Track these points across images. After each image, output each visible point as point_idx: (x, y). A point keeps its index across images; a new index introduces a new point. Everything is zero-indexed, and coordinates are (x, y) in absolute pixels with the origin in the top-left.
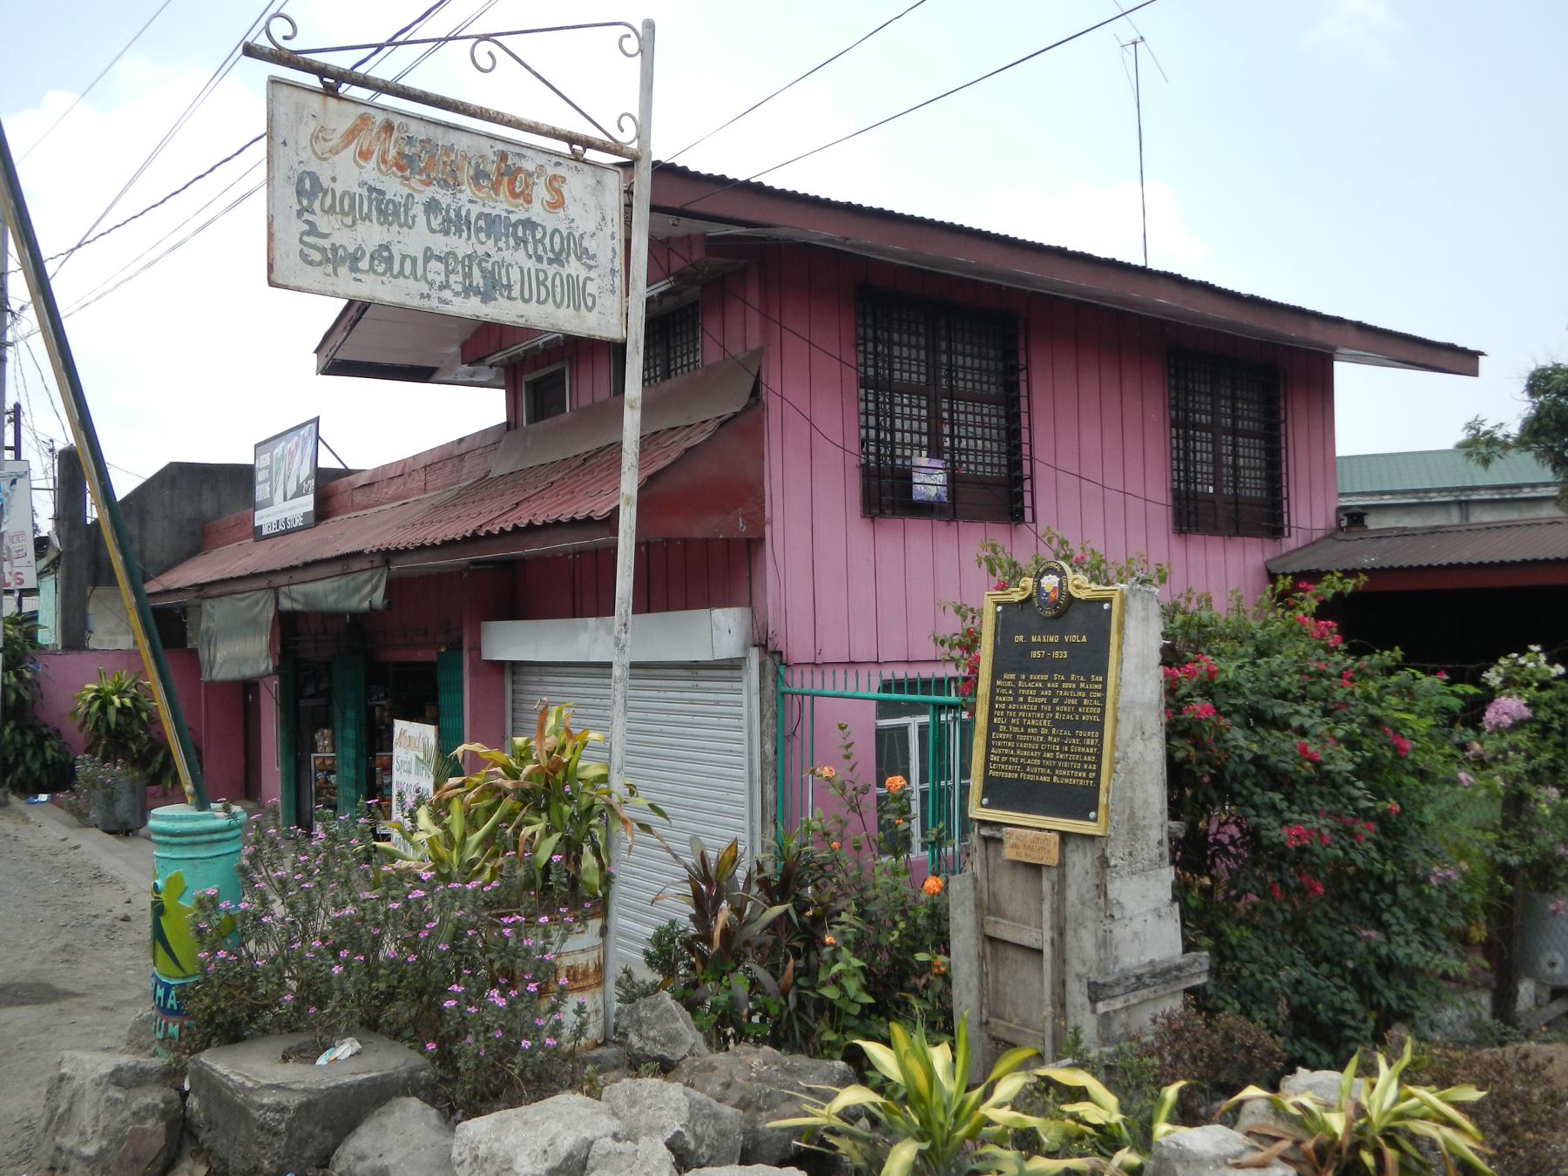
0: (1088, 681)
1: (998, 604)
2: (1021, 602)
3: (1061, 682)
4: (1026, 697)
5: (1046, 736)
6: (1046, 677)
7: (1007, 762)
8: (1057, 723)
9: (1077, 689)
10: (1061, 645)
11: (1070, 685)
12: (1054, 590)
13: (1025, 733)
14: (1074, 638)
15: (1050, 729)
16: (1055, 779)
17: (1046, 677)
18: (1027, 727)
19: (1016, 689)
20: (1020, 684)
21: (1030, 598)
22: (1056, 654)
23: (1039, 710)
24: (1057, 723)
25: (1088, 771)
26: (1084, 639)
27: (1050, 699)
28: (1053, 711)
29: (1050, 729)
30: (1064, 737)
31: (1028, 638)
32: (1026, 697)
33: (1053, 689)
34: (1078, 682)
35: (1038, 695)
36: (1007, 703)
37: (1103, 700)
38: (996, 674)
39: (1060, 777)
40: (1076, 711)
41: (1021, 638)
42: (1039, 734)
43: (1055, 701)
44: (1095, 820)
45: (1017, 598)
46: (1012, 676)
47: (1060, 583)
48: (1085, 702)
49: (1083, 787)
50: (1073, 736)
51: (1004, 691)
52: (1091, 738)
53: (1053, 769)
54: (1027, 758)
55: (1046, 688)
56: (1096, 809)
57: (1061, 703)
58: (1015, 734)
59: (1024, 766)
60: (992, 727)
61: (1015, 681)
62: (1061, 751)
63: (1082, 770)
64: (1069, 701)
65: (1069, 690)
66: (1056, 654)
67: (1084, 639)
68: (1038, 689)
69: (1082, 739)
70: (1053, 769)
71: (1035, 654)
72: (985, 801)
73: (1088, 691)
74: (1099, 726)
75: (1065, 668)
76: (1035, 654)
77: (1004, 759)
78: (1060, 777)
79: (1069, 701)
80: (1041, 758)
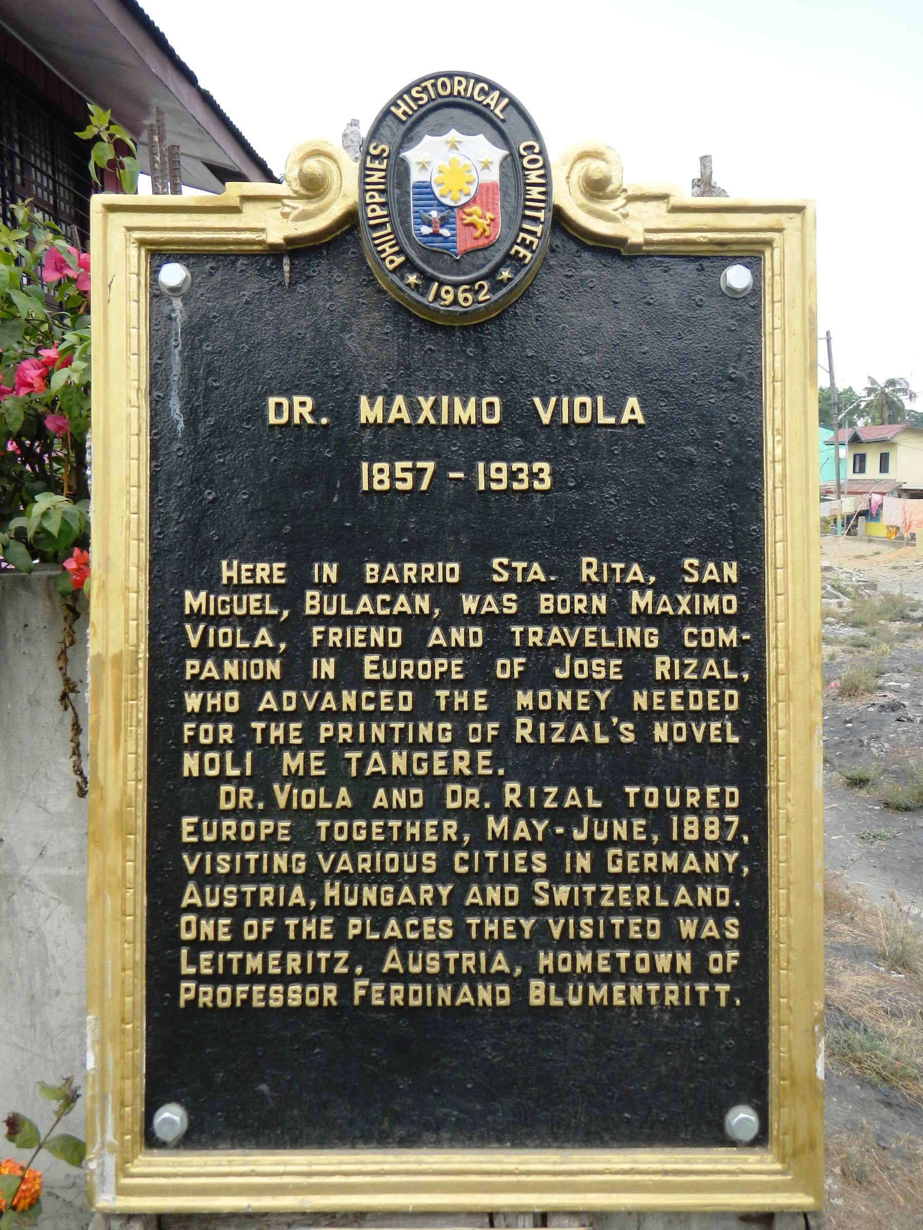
0: (669, 581)
1: (158, 254)
2: (300, 250)
3: (528, 592)
4: (349, 658)
5: (471, 820)
6: (451, 571)
7: (278, 940)
8: (532, 763)
9: (619, 615)
10: (519, 434)
11: (582, 610)
12: (482, 194)
13: (362, 808)
14: (582, 408)
15: (492, 788)
16: (537, 993)
17: (451, 571)
18: (364, 787)
19: (293, 630)
20: (312, 602)
21: (350, 222)
22: (494, 475)
23: (425, 708)
24: (532, 763)
25: (699, 948)
26: (633, 410)
27: (478, 668)
28: (502, 707)
29: (492, 788)
30: (571, 817)
31: (338, 405)
32: (349, 658)
33: (496, 625)
34: (619, 594)
35: (415, 646)
36: (250, 690)
37: (750, 658)
38: (179, 557)
39: (559, 980)
40: (621, 705)
41: (302, 408)
42: (435, 807)
43: (508, 668)
44: (761, 1139)
45: (275, 226)
46: (270, 571)
47: (513, 166)
48: (662, 666)
49: (677, 1012)
50: (614, 807)
51: (225, 637)
52: (707, 812)
53: (522, 951)
54: (379, 915)
55: (453, 617)
56: (758, 1096)
57: (541, 669)
58: (303, 820)
59: (368, 954)
60: (171, 795)
61: (288, 594)
62: (555, 874)
63: (671, 940)
64: (581, 668)
65: (571, 620)
66: (494, 475)
67: (633, 410)
68: (415, 628)
69: (659, 819)
70: (522, 951)
71: (377, 476)
72: (172, 1117)
73: (670, 626)
74: (746, 765)
75: (554, 533)
76: (377, 476)
77: (252, 929)
78: (559, 980)
79: (581, 668)
80: (456, 909)
